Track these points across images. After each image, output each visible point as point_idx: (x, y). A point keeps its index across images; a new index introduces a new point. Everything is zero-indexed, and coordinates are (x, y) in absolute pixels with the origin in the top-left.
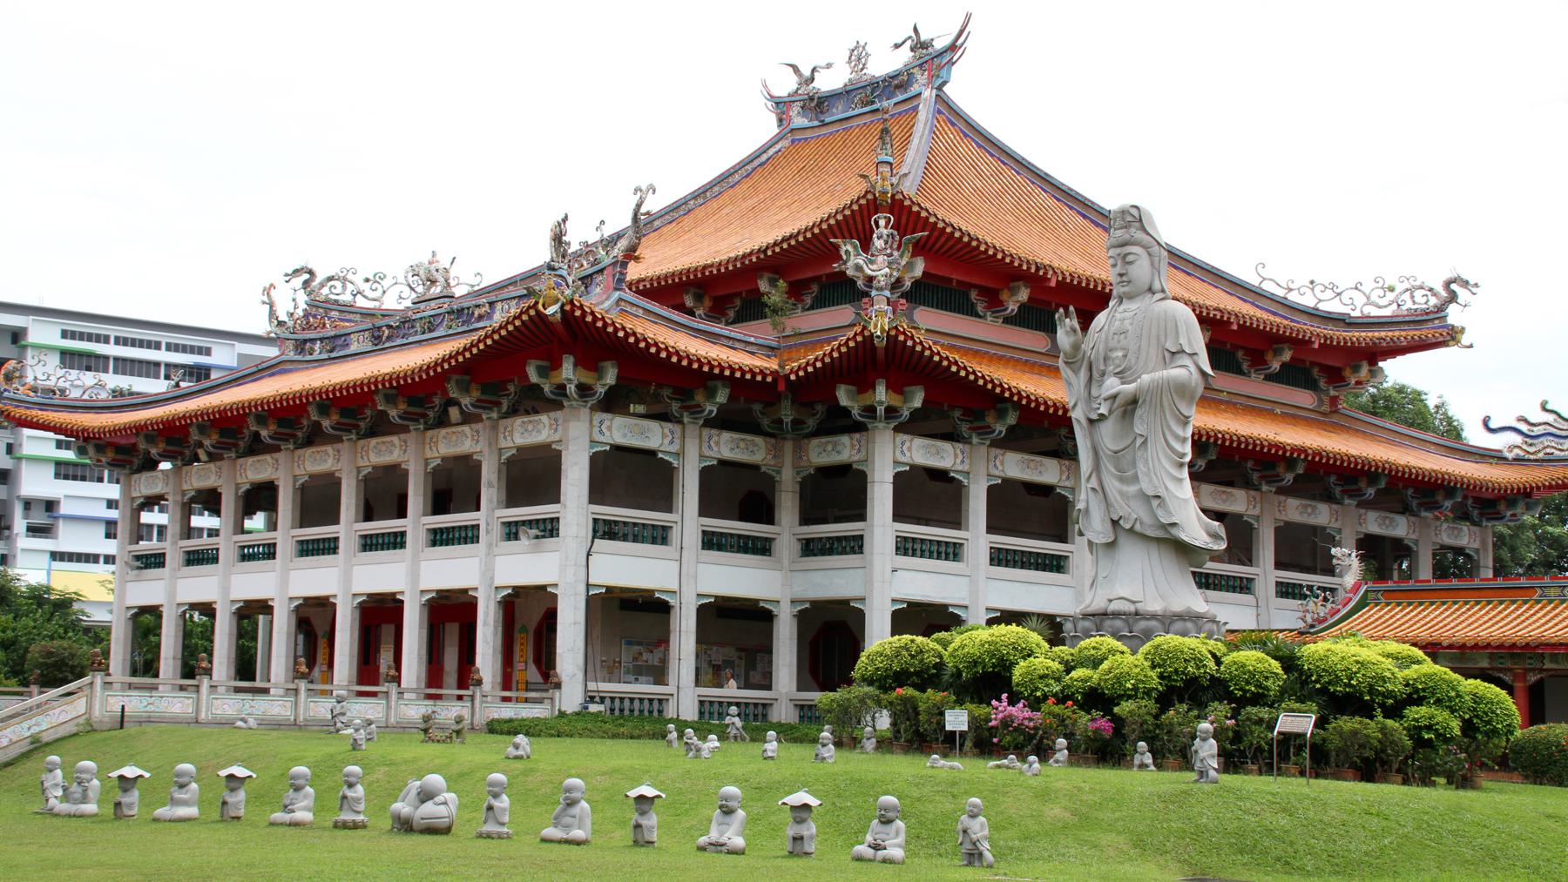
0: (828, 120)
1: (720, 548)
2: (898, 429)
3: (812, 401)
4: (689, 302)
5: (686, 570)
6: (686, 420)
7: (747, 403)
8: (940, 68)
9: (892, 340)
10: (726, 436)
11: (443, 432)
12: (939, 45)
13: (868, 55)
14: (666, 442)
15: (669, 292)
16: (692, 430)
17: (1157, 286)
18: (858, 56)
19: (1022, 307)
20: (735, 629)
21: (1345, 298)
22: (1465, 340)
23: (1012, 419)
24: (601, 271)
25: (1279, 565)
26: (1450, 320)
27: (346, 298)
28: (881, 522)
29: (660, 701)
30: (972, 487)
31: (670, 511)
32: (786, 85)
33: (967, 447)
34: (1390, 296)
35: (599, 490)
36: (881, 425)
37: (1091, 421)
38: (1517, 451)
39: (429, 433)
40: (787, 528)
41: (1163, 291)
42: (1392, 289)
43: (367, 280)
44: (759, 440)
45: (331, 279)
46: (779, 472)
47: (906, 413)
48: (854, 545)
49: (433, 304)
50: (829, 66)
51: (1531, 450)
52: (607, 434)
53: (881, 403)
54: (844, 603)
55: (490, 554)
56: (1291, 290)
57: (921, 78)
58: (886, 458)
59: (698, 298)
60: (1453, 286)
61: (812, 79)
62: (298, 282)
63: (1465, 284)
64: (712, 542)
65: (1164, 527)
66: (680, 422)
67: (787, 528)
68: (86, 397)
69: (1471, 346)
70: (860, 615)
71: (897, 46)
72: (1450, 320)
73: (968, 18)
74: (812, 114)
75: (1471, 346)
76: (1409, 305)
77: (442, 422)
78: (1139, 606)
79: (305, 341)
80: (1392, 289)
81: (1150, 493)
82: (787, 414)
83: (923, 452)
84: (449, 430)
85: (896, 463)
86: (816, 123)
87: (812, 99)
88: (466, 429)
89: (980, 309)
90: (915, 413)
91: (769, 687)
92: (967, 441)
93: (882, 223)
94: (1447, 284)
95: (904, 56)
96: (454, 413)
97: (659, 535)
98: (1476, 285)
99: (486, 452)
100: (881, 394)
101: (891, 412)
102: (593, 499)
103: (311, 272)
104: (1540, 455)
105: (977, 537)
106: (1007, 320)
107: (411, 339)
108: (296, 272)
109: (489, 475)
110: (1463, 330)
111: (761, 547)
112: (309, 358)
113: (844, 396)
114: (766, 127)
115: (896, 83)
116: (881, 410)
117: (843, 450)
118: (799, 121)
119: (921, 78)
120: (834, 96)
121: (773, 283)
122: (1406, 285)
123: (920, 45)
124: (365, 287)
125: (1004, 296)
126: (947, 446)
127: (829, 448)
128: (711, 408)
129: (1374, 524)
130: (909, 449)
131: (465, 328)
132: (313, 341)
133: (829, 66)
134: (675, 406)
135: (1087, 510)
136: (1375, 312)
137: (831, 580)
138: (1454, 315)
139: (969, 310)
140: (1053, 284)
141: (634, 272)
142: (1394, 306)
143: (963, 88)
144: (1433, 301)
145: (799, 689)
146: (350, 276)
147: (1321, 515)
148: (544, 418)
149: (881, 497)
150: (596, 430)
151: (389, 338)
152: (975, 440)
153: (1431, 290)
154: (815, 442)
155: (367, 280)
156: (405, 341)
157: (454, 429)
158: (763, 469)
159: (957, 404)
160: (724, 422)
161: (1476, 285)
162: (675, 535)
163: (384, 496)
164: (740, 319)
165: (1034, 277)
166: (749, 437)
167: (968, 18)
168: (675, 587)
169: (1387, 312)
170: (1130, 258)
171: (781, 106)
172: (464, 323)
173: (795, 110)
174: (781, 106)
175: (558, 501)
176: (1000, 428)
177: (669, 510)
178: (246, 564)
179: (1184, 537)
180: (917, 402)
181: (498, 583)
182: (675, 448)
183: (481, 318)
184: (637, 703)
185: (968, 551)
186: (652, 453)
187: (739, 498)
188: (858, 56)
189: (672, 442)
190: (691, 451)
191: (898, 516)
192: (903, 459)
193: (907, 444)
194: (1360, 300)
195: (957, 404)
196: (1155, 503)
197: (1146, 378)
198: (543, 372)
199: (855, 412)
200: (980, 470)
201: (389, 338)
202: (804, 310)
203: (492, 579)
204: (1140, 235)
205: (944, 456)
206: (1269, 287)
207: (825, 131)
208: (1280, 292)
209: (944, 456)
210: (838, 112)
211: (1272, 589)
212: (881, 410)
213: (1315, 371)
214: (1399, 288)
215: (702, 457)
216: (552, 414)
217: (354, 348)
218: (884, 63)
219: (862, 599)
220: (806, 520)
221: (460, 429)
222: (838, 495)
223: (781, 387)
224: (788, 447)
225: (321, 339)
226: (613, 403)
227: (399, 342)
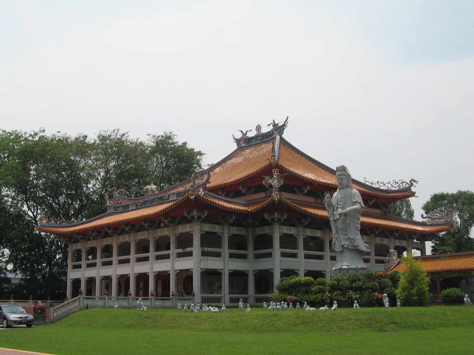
0: (251, 144)
1: (234, 257)
2: (280, 224)
3: (258, 219)
4: (220, 193)
5: (225, 264)
6: (224, 224)
7: (240, 219)
8: (280, 130)
9: (279, 200)
10: (235, 228)
11: (159, 230)
12: (280, 125)
13: (261, 128)
14: (220, 230)
15: (216, 190)
16: (226, 227)
17: (349, 185)
18: (258, 128)
19: (308, 191)
20: (239, 278)
21: (386, 185)
22: (416, 195)
23: (309, 220)
25: (376, 255)
26: (412, 190)
28: (277, 250)
29: (220, 299)
30: (299, 238)
31: (221, 248)
32: (239, 136)
33: (297, 228)
34: (397, 185)
35: (203, 244)
36: (276, 223)
37: (335, 220)
38: (430, 223)
39: (155, 230)
40: (251, 251)
41: (351, 187)
42: (397, 183)
44: (243, 229)
46: (248, 237)
47: (282, 220)
48: (270, 255)
49: (152, 196)
50: (251, 131)
51: (433, 222)
52: (204, 229)
53: (276, 217)
54: (267, 271)
55: (173, 261)
56: (372, 184)
58: (277, 232)
59: (222, 192)
60: (412, 182)
61: (246, 134)
63: (415, 181)
64: (231, 256)
65: (355, 246)
66: (223, 225)
67: (251, 251)
69: (417, 197)
70: (272, 273)
71: (269, 125)
72: (412, 190)
73: (287, 118)
74: (245, 143)
75: (417, 197)
76: (402, 187)
77: (159, 227)
78: (350, 267)
79: (117, 207)
80: (397, 183)
81: (351, 237)
82: (250, 221)
83: (286, 230)
84: (161, 229)
85: (280, 233)
86: (248, 145)
87: (246, 139)
88: (166, 229)
89: (297, 192)
90: (285, 220)
91: (247, 294)
92: (297, 227)
93: (276, 171)
94: (410, 181)
95: (271, 127)
96: (162, 224)
97: (218, 255)
98: (417, 181)
99: (171, 234)
100: (276, 215)
101: (279, 220)
104: (435, 224)
105: (301, 252)
106: (304, 195)
107: (146, 206)
109: (172, 240)
110: (415, 193)
111: (244, 257)
112: (117, 211)
113: (266, 216)
114: (235, 147)
116: (276, 219)
117: (266, 230)
118: (243, 145)
121: (243, 187)
122: (401, 182)
123: (275, 125)
125: (303, 188)
126: (292, 228)
127: (262, 230)
128: (231, 221)
129: (398, 243)
130: (283, 229)
132: (119, 207)
133: (251, 131)
134: (221, 221)
135: (335, 243)
136: (394, 189)
137: (264, 264)
138: (413, 189)
139: (294, 192)
140: (316, 185)
141: (208, 185)
142: (398, 187)
143: (287, 135)
144: (407, 186)
145: (255, 294)
147: (386, 241)
148: (188, 225)
150: (202, 228)
151: (140, 206)
152: (299, 226)
153: (407, 183)
154: (258, 228)
156: (144, 206)
157: (162, 229)
158: (244, 236)
160: (234, 224)
161: (417, 181)
162: (222, 255)
163: (143, 247)
164: (233, 197)
166: (241, 228)
167: (287, 118)
168: (222, 268)
169: (397, 189)
170: (342, 179)
173: (242, 142)
174: (238, 141)
175: (192, 246)
176: (306, 223)
177: (221, 248)
179: (360, 249)
180: (285, 217)
181: (176, 269)
182: (222, 231)
183: (166, 199)
184: (214, 299)
185: (299, 255)
186: (216, 233)
187: (238, 244)
188: (258, 128)
189: (221, 230)
190: (226, 233)
191: (281, 247)
192: (282, 232)
193: (283, 228)
194: (390, 186)
195: (296, 218)
196: (352, 240)
197: (349, 209)
198: (188, 213)
199: (269, 220)
200: (301, 234)
201: (140, 206)
202: (251, 194)
203: (174, 268)
204: (344, 173)
205: (292, 231)
206: (367, 183)
208: (370, 185)
209: (292, 231)
211: (374, 261)
212: (276, 219)
213: (380, 205)
214: (399, 182)
215: (229, 234)
216: (190, 224)
217: (130, 208)
218: (265, 129)
219: (272, 269)
220: (255, 249)
222: (264, 242)
223: (250, 215)
224: (250, 230)
225: (121, 207)
226: (206, 220)
227: (143, 206)
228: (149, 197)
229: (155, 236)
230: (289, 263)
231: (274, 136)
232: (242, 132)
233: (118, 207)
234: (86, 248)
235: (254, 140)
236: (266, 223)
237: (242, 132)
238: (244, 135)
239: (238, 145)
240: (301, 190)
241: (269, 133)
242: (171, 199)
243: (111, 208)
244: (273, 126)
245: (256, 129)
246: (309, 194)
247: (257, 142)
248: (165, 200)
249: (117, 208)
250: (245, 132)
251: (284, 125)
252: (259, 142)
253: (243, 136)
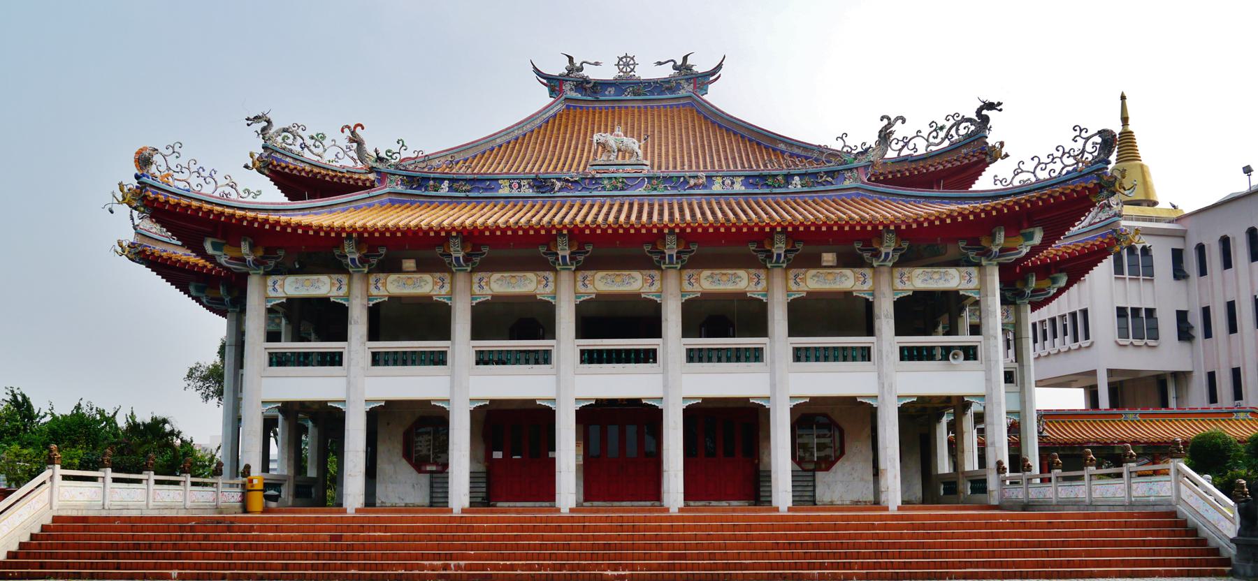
11: (813, 272)
18: (626, 62)
24: (851, 169)
27: (297, 148)
32: (557, 68)
43: (312, 138)
45: (285, 130)
49: (629, 168)
50: (597, 64)
61: (582, 69)
62: (259, 126)
68: (217, 194)
71: (660, 63)
88: (847, 272)
95: (667, 72)
102: (898, 332)
103: (269, 122)
108: (257, 118)
120: (604, 84)
123: (683, 68)
124: (309, 142)
131: (675, 192)
133: (597, 64)
146: (300, 132)
151: (561, 189)
155: (312, 138)
171: (554, 84)
172: (674, 188)
174: (554, 84)
178: (481, 367)
188: (626, 62)
201: (561, 189)
207: (597, 105)
210: (610, 93)
217: (504, 191)
218: (646, 71)
221: (837, 271)
228: (612, 168)
229: (794, 287)
231: (682, 93)
232: (571, 59)
233: (434, 179)
234: (370, 297)
235: (612, 90)
237: (571, 59)
238: (573, 68)
239: (553, 92)
241: (667, 81)
242: (717, 188)
243: (393, 178)
244: (675, 67)
245: (618, 65)
247: (623, 97)
248: (691, 188)
249: (431, 183)
250: (577, 63)
252: (629, 97)
253: (570, 71)
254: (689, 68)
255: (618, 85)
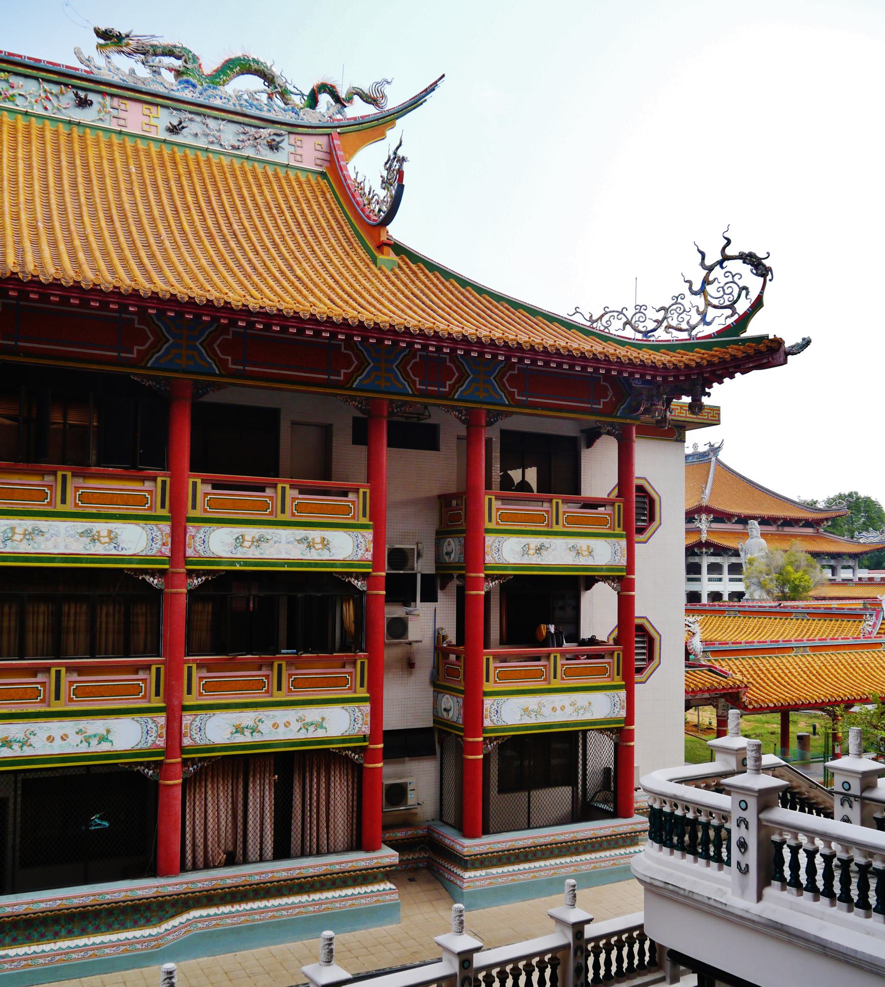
12: (716, 446)
48: (698, 580)
57: (712, 454)
58: (706, 561)
95: (707, 448)
101: (706, 553)
105: (726, 576)
115: (704, 455)
117: (696, 560)
119: (712, 454)
123: (711, 446)
143: (722, 456)
149: (704, 569)
159: (719, 550)
165: (739, 516)
195: (719, 550)
200: (725, 562)
230: (715, 587)
236: (696, 554)
240: (729, 520)
241: (705, 453)
246: (736, 522)
251: (719, 447)
254: (713, 446)
255: (692, 455)
